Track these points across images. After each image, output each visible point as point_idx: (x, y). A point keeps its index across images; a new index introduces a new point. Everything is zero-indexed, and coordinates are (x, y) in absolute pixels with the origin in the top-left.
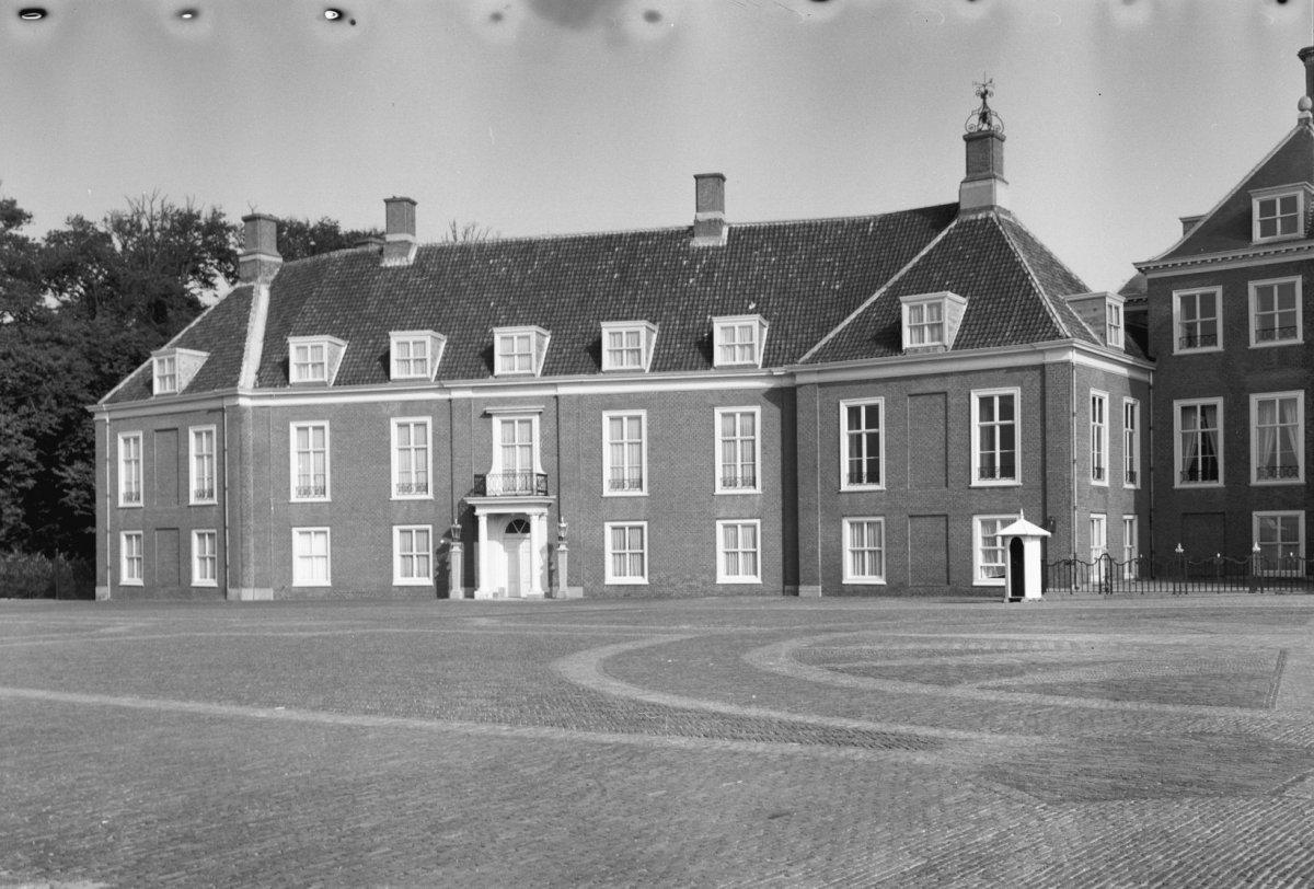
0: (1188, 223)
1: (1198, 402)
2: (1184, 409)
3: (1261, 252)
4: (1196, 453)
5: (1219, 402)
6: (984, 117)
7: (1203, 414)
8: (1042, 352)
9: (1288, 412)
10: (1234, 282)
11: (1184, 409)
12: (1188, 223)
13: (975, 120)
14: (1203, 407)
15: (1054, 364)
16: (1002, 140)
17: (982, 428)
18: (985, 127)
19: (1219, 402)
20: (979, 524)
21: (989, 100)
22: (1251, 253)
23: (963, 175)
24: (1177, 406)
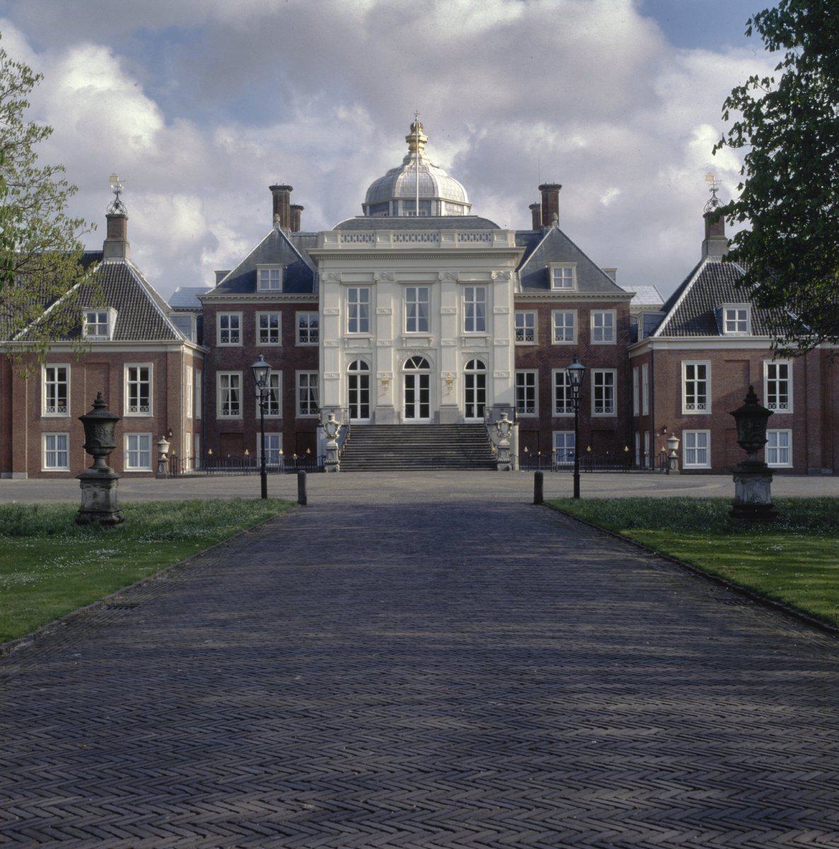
0: (220, 275)
1: (230, 374)
2: (222, 376)
3: (277, 297)
4: (228, 400)
5: (240, 374)
6: (117, 206)
7: (311, 379)
8: (166, 345)
9: (234, 383)
10: (249, 311)
11: (222, 376)
12: (220, 275)
13: (112, 207)
14: (232, 376)
15: (172, 353)
16: (127, 219)
17: (48, 385)
18: (117, 212)
19: (240, 374)
20: (127, 438)
21: (120, 196)
22: (258, 297)
23: (105, 237)
24: (219, 374)
